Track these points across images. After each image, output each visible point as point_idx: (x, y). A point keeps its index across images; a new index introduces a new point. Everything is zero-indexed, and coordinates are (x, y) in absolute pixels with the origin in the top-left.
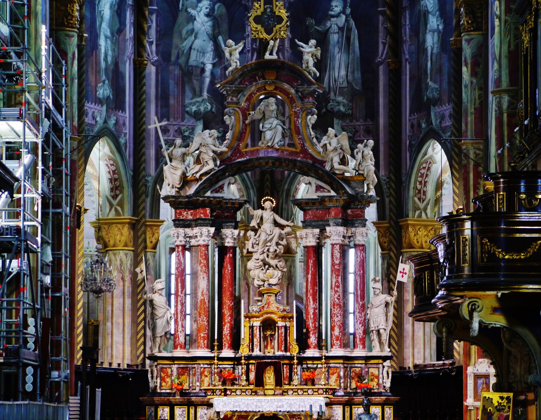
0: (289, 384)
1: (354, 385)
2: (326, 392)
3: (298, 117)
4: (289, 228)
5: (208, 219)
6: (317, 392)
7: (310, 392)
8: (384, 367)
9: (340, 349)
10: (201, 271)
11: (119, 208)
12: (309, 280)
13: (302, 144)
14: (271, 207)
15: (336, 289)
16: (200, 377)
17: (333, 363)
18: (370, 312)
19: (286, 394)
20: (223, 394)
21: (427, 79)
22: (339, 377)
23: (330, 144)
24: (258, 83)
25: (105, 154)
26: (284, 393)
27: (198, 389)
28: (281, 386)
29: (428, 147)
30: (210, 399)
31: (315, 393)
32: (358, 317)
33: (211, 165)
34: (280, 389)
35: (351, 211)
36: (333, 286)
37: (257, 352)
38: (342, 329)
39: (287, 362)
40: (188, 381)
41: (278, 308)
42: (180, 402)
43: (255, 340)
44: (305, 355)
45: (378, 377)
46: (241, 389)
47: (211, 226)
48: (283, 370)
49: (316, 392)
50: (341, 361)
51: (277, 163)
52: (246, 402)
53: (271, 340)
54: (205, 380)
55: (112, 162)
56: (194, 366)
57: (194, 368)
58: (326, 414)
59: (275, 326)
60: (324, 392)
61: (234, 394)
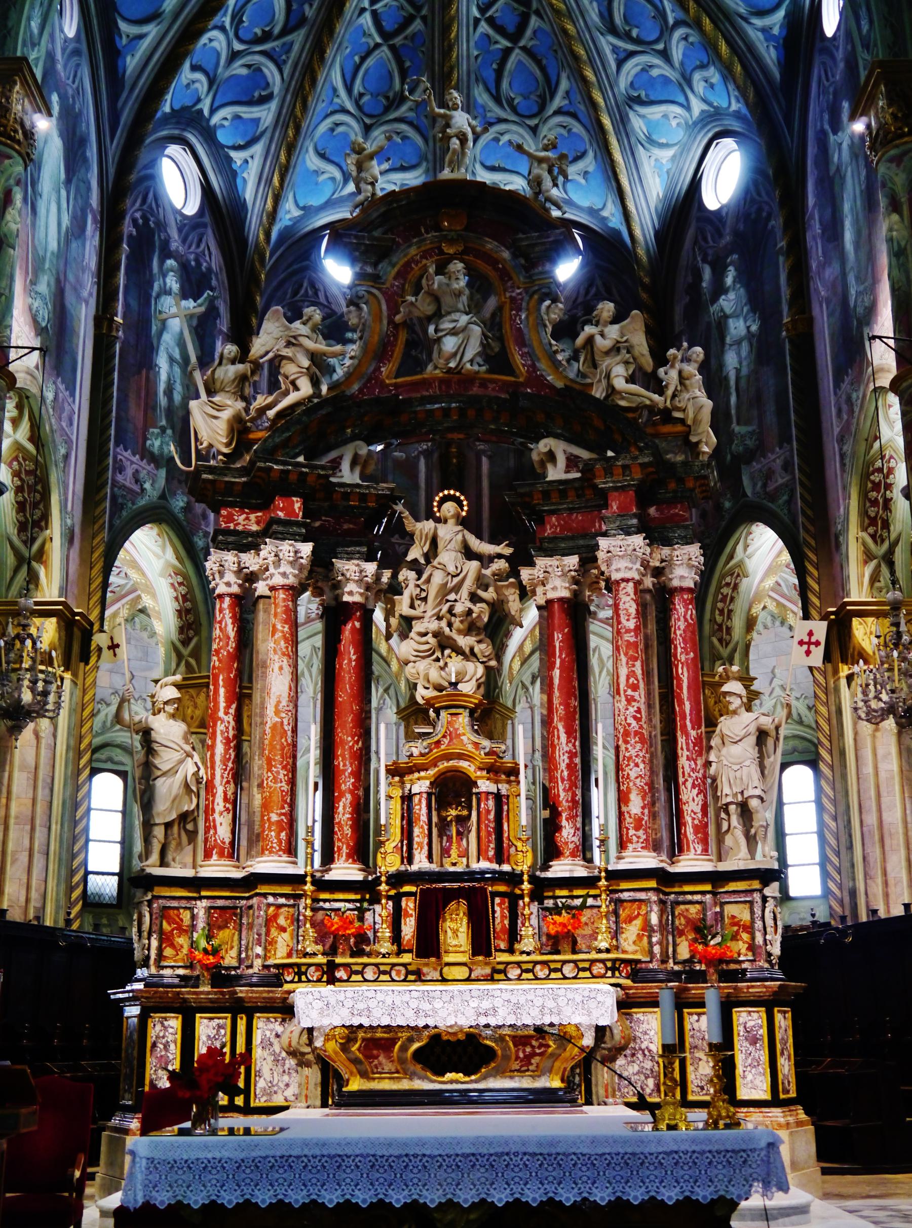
0: (511, 951)
1: (684, 952)
2: (613, 969)
3: (519, 309)
4: (503, 561)
5: (297, 524)
6: (589, 969)
7: (568, 970)
8: (764, 899)
9: (645, 853)
10: (275, 651)
11: (192, 661)
12: (556, 681)
13: (528, 366)
14: (457, 516)
15: (629, 692)
16: (264, 929)
17: (627, 890)
18: (718, 757)
19: (502, 976)
20: (325, 979)
21: (731, 423)
22: (647, 927)
23: (602, 335)
24: (425, 240)
25: (169, 564)
26: (497, 974)
27: (258, 963)
28: (488, 954)
29: (737, 543)
30: (289, 992)
31: (581, 974)
32: (687, 770)
33: (305, 388)
34: (487, 964)
35: (657, 510)
36: (622, 686)
37: (421, 863)
38: (648, 799)
39: (502, 888)
40: (236, 943)
41: (476, 745)
42: (211, 1001)
43: (416, 831)
44: (549, 874)
45: (750, 929)
46: (376, 965)
47: (305, 540)
48: (494, 912)
49: (585, 970)
50: (653, 884)
51: (471, 413)
52: (389, 1001)
53: (459, 834)
54: (280, 939)
55: (180, 579)
56: (251, 902)
57: (251, 907)
58: (615, 1031)
59: (471, 794)
60: (607, 969)
61: (359, 978)
